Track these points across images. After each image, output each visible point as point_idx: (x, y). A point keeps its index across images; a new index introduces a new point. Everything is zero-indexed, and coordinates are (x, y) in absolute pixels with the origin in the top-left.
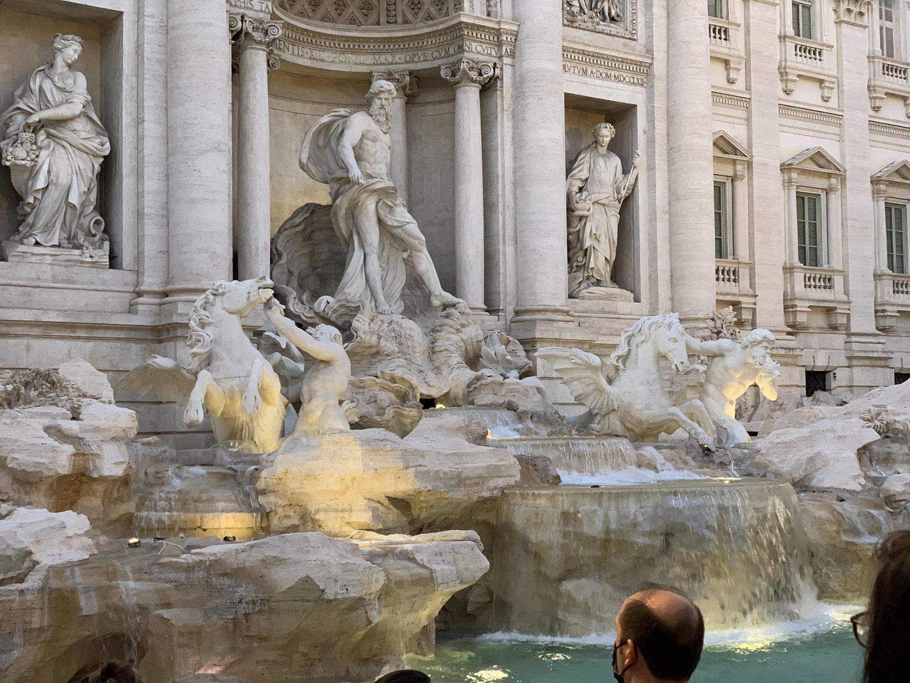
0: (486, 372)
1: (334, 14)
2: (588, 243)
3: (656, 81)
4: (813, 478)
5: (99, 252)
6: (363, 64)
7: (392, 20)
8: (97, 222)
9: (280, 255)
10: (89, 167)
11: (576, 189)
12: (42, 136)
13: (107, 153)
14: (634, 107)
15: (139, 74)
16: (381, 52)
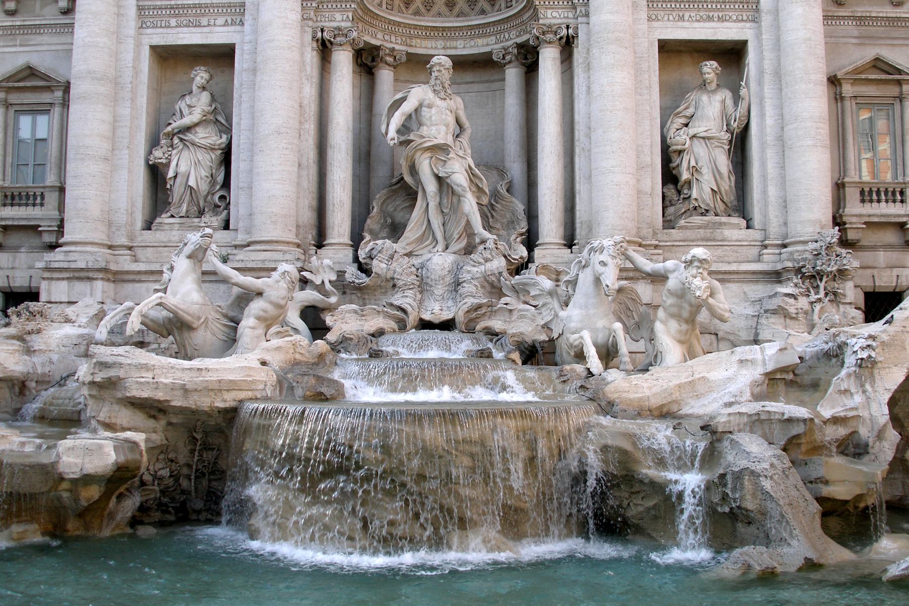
0: (504, 300)
1: (467, 9)
2: (685, 176)
3: (763, 14)
4: (686, 404)
5: (214, 219)
6: (488, 45)
7: (509, 4)
8: (222, 198)
9: (373, 208)
10: (208, 160)
11: (676, 126)
12: (176, 140)
13: (223, 146)
14: (745, 43)
15: (241, 85)
16: (500, 32)
